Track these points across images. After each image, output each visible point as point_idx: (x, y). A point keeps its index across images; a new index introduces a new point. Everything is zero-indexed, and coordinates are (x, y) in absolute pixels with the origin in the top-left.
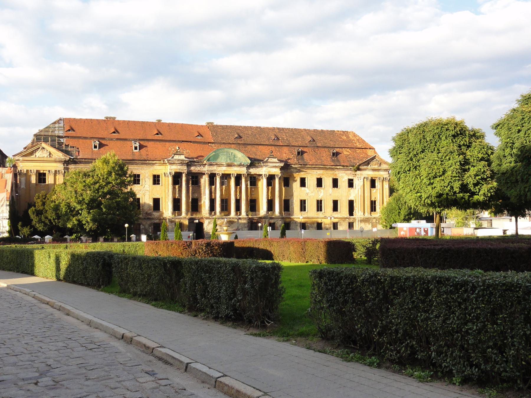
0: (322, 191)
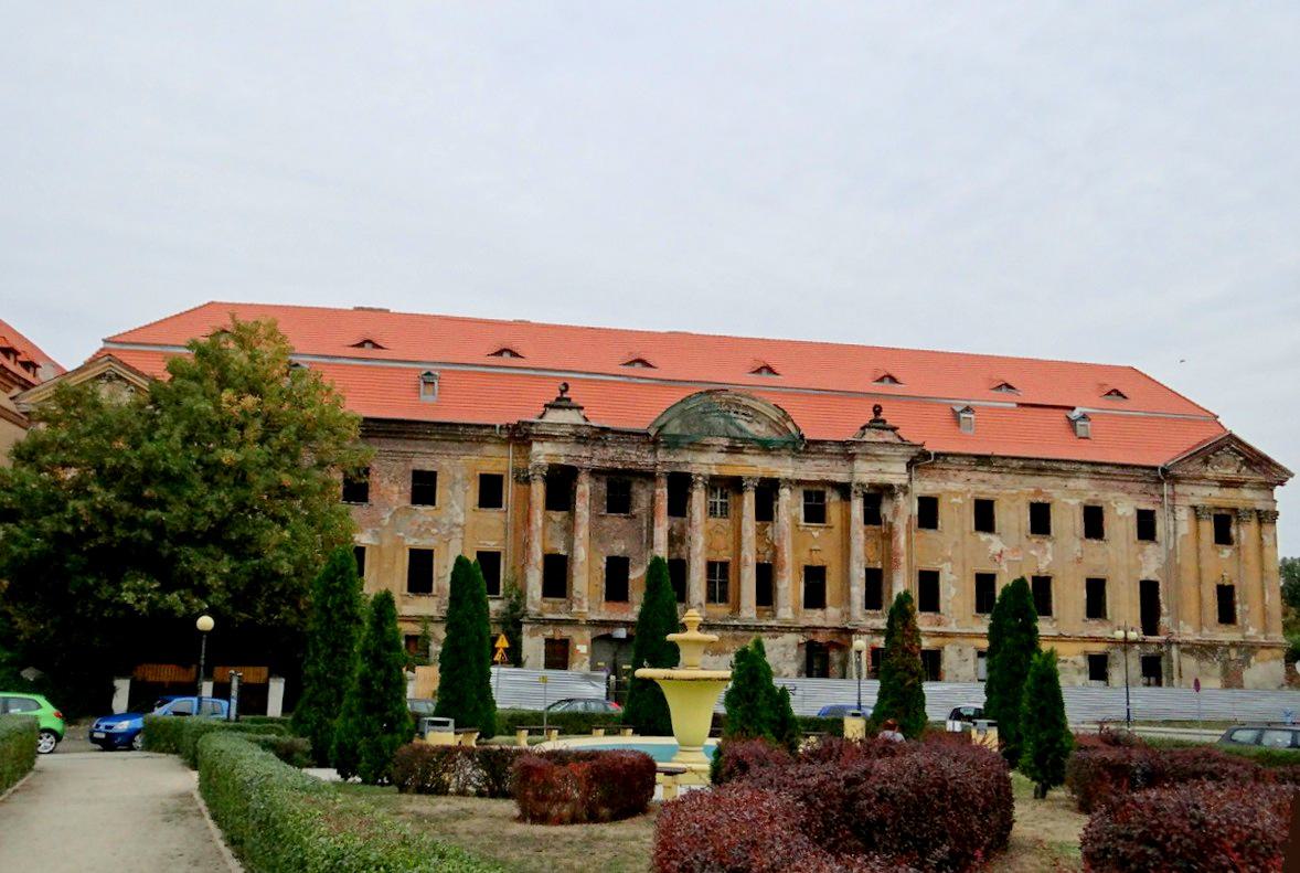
0: (1049, 545)
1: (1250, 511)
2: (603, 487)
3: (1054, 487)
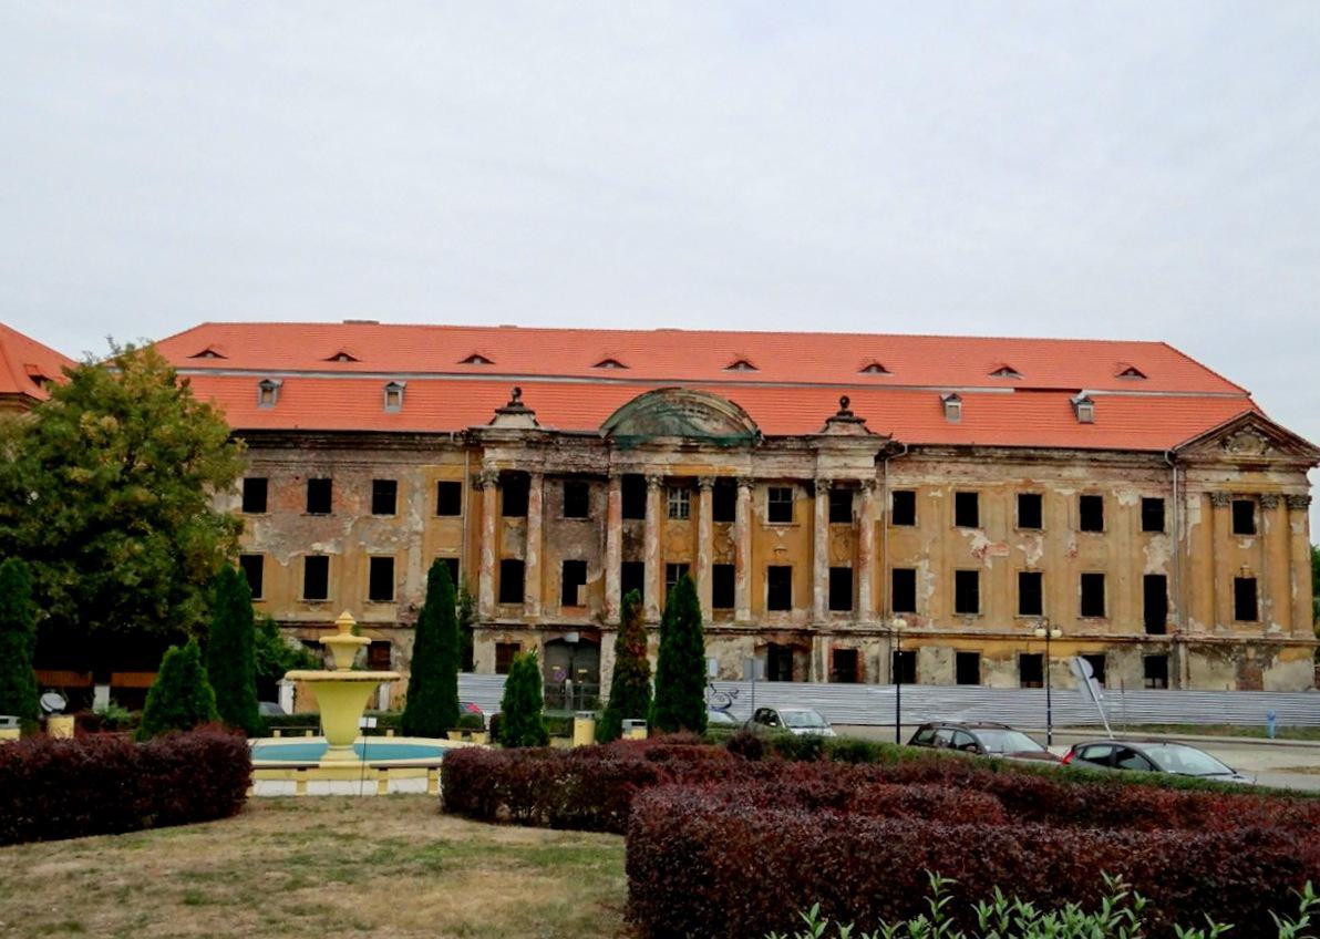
0: (1039, 539)
1: (1277, 497)
2: (560, 491)
3: (1047, 477)
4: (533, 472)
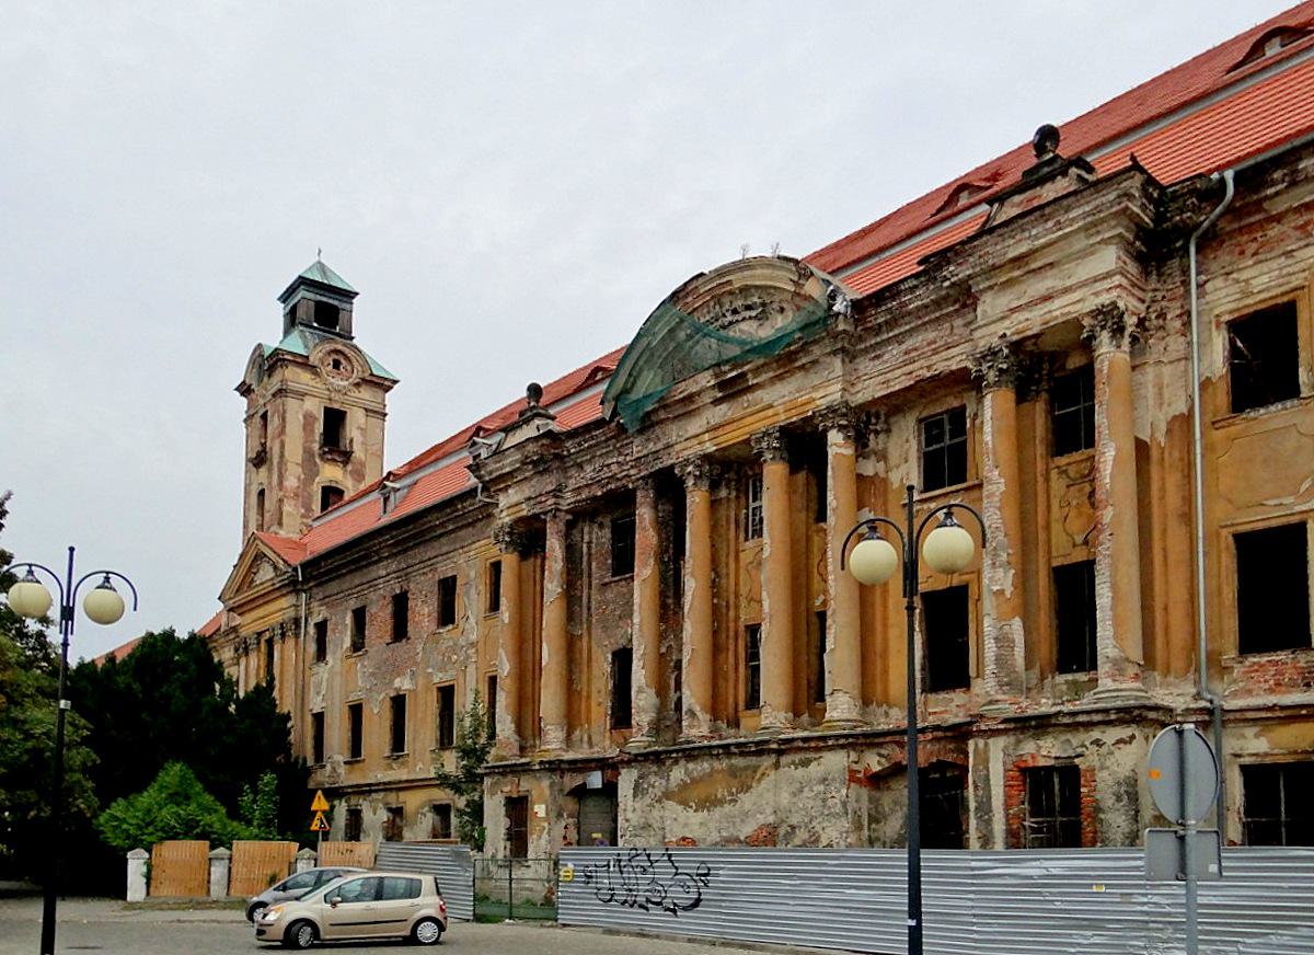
4: (545, 513)
